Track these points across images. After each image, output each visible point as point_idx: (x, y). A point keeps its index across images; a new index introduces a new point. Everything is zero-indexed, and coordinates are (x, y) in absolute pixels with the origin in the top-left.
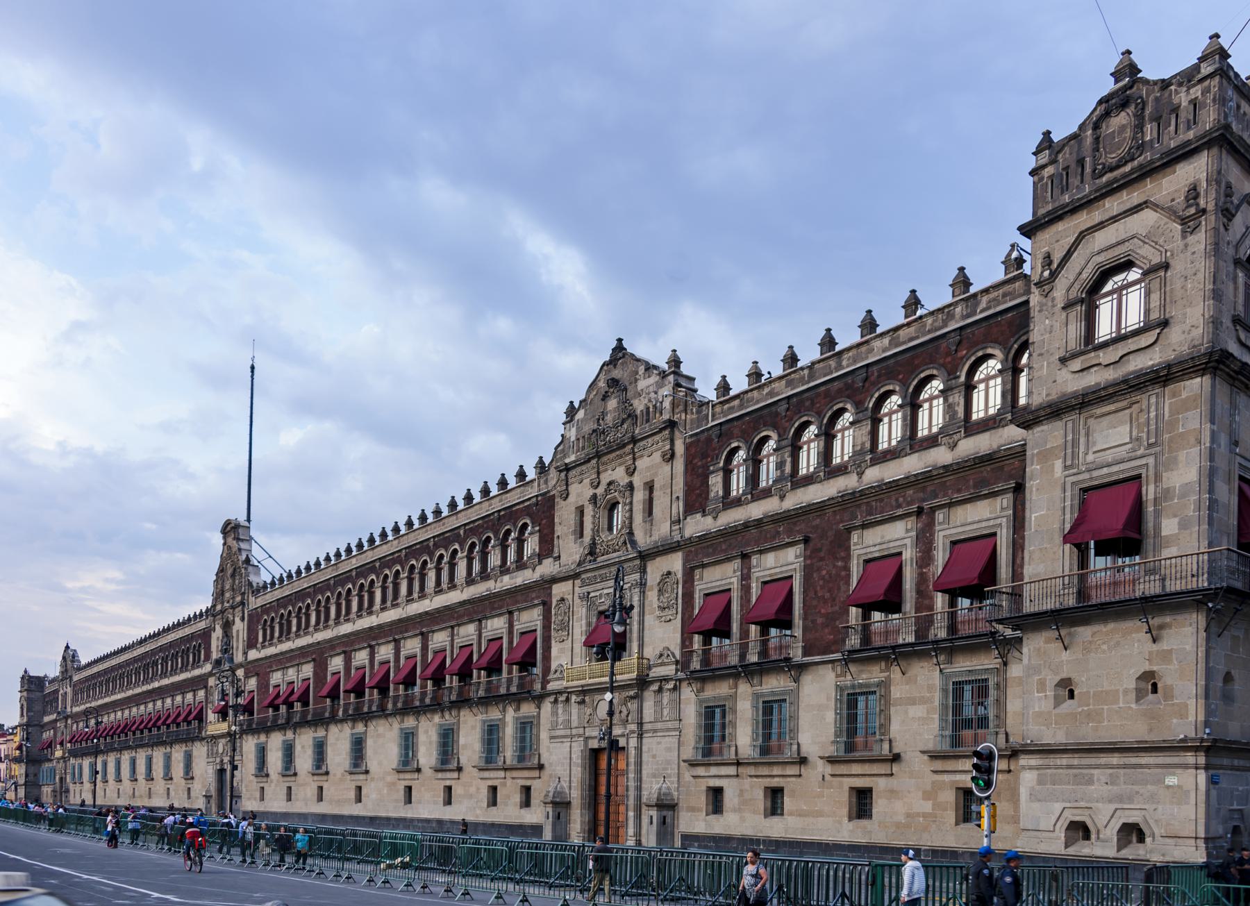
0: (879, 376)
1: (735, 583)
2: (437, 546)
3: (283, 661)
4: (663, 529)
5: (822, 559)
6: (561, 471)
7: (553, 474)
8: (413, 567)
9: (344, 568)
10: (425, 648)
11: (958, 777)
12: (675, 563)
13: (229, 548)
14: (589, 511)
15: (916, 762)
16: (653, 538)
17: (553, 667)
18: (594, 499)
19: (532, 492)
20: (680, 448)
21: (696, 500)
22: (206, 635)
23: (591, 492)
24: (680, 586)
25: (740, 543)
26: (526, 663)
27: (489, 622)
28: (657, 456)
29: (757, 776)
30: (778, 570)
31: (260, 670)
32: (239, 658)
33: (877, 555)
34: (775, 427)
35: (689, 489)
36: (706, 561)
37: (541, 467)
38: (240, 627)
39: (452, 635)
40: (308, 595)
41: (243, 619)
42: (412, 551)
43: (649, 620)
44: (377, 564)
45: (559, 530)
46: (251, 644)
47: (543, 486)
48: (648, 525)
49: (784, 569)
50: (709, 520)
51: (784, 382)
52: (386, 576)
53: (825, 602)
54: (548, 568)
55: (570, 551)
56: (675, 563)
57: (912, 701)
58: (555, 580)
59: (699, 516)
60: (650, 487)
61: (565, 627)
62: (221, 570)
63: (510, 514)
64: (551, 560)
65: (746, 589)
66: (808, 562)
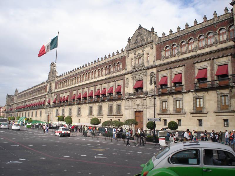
0: (199, 32)
1: (169, 75)
2: (98, 67)
3: (63, 91)
4: (151, 63)
5: (188, 70)
6: (127, 51)
7: (125, 52)
8: (93, 72)
9: (77, 72)
10: (95, 89)
11: (222, 117)
13: (52, 68)
14: (134, 61)
16: (149, 65)
17: (125, 93)
18: (135, 57)
19: (121, 55)
20: (154, 46)
21: (159, 57)
22: (46, 87)
23: (134, 55)
25: (170, 66)
26: (119, 93)
27: (110, 83)
28: (149, 48)
30: (178, 72)
31: (58, 94)
32: (53, 91)
33: (201, 68)
34: (176, 42)
35: (157, 55)
37: (122, 51)
38: (53, 85)
39: (102, 86)
40: (69, 78)
41: (54, 83)
42: (93, 68)
44: (85, 71)
45: (127, 64)
46: (56, 88)
47: (123, 54)
49: (180, 71)
50: (162, 61)
51: (178, 33)
52: (87, 74)
54: (124, 72)
55: (129, 68)
56: (154, 70)
58: (125, 74)
59: (159, 60)
60: (148, 54)
61: (128, 84)
62: (50, 73)
63: (115, 60)
65: (171, 76)
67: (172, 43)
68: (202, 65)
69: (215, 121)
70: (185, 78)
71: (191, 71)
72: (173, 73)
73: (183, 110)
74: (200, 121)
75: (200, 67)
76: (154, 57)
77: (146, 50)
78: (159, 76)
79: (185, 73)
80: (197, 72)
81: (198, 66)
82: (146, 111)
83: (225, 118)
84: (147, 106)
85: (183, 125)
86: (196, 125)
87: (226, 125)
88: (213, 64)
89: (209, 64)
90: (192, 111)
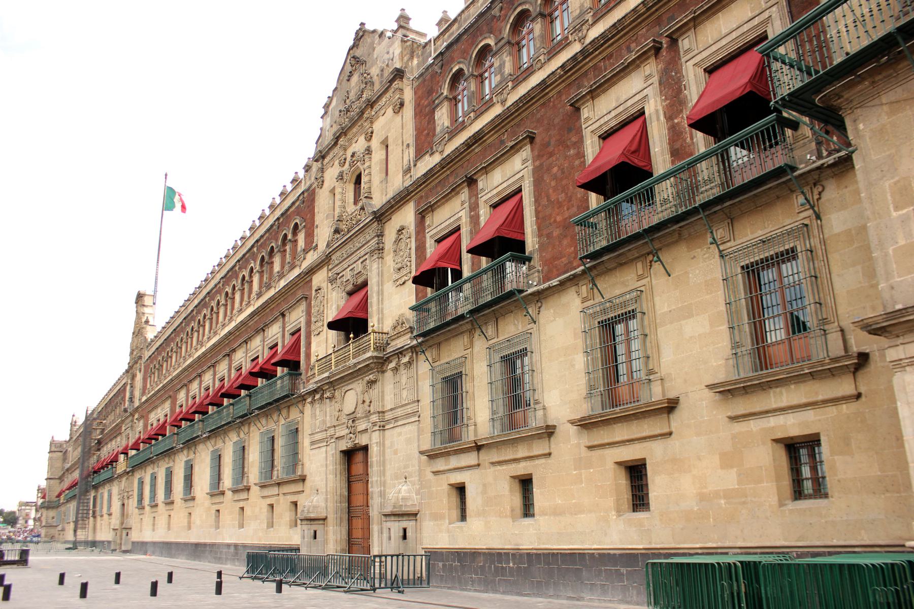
5: (551, 155)
12: (407, 216)
15: (700, 410)
20: (408, 95)
24: (413, 239)
29: (500, 463)
36: (432, 200)
43: (389, 287)
48: (384, 183)
53: (560, 205)
57: (687, 313)
64: (312, 251)
66: (537, 163)
67: (473, 43)
68: (617, 101)
69: (728, 460)
70: (537, 212)
71: (566, 157)
72: (481, 202)
73: (540, 413)
74: (636, 473)
75: (606, 119)
76: (408, 145)
77: (378, 126)
78: (428, 236)
79: (538, 183)
80: (591, 148)
81: (600, 112)
82: (382, 444)
83: (794, 425)
84: (388, 416)
85: (544, 514)
86: (610, 502)
87: (808, 486)
88: (679, 71)
89: (655, 80)
90: (584, 410)
